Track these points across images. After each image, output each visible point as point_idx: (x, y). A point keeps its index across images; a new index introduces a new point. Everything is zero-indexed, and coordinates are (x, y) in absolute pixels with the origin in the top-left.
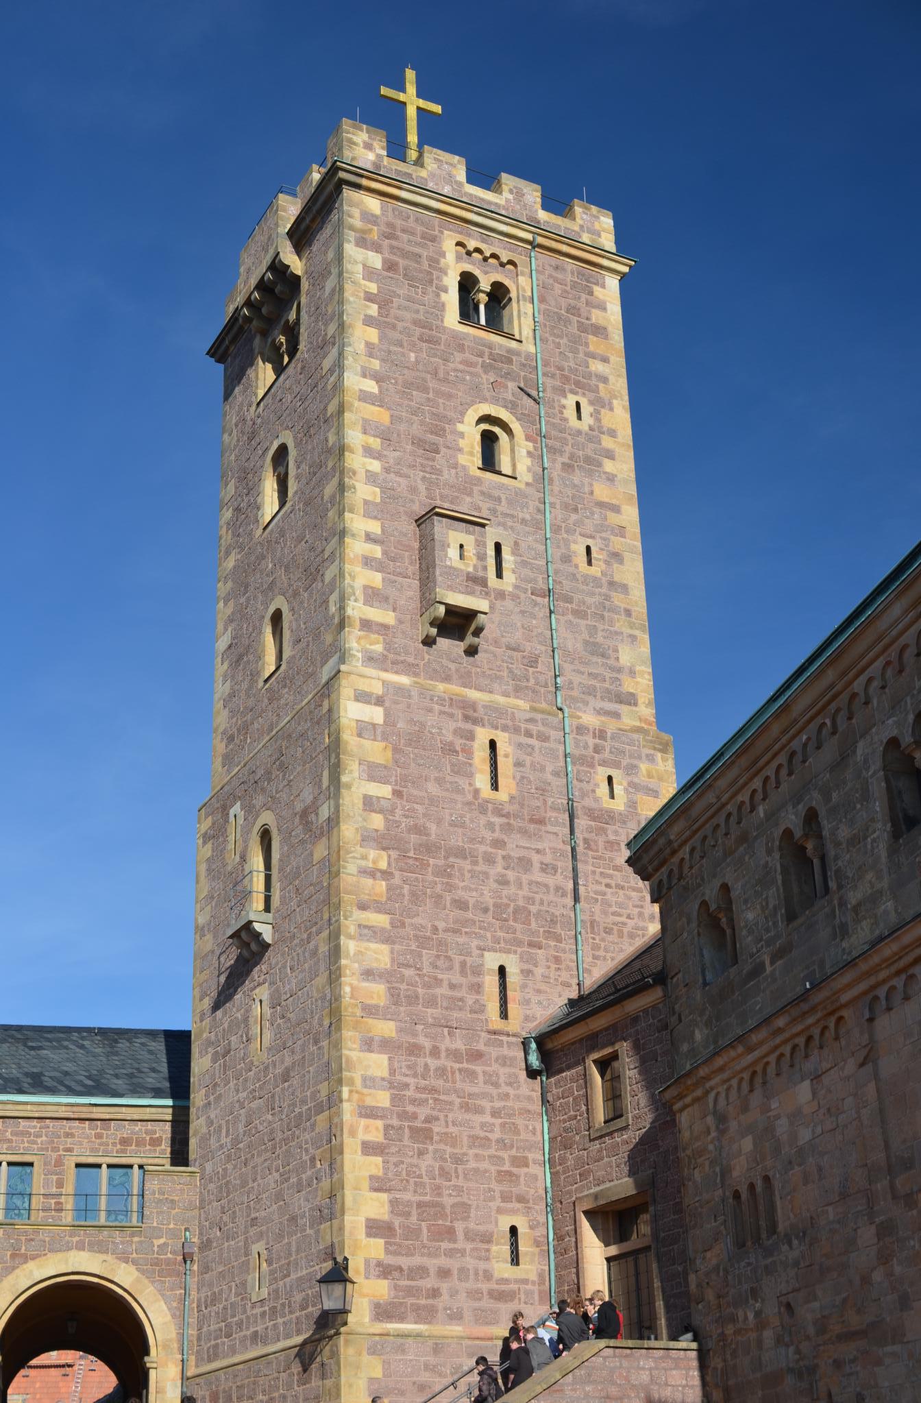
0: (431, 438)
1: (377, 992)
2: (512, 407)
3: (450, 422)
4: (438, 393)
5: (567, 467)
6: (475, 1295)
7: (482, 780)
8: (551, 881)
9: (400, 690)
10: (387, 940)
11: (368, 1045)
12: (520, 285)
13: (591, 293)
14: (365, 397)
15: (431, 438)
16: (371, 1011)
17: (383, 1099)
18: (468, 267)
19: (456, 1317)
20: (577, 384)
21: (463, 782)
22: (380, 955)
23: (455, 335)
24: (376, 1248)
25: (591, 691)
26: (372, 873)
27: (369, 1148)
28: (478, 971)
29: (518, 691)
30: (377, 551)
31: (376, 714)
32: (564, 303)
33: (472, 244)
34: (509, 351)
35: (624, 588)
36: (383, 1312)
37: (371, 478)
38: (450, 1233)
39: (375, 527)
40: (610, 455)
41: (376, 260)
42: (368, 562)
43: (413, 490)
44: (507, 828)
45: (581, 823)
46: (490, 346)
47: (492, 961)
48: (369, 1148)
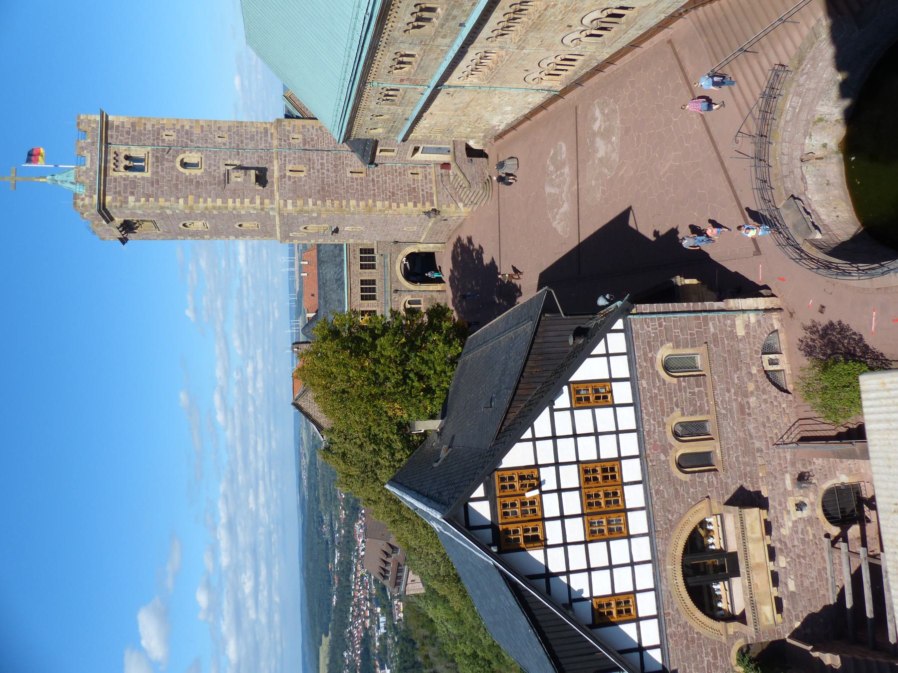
0: (194, 183)
1: (362, 203)
2: (175, 157)
3: (186, 177)
4: (177, 180)
5: (192, 141)
6: (426, 183)
7: (302, 175)
8: (325, 158)
9: (280, 195)
10: (348, 201)
11: (375, 206)
12: (123, 150)
13: (118, 126)
14: (186, 202)
15: (194, 183)
16: (367, 205)
17: (387, 203)
18: (122, 169)
19: (431, 188)
20: (158, 134)
21: (303, 179)
22: (353, 203)
23: (153, 173)
24: (419, 205)
25: (266, 141)
26: (333, 204)
27: (398, 206)
28: (352, 179)
29: (271, 162)
30: (238, 200)
31: (290, 202)
32: (126, 136)
33: (113, 166)
34: (153, 156)
35: (229, 127)
36: (432, 203)
37: (214, 201)
38: (414, 188)
39: (230, 201)
40: (183, 127)
41: (131, 199)
42: (242, 203)
43: (214, 189)
44: (313, 168)
45: (307, 147)
46: (153, 163)
47: (349, 175)
48: (398, 206)
